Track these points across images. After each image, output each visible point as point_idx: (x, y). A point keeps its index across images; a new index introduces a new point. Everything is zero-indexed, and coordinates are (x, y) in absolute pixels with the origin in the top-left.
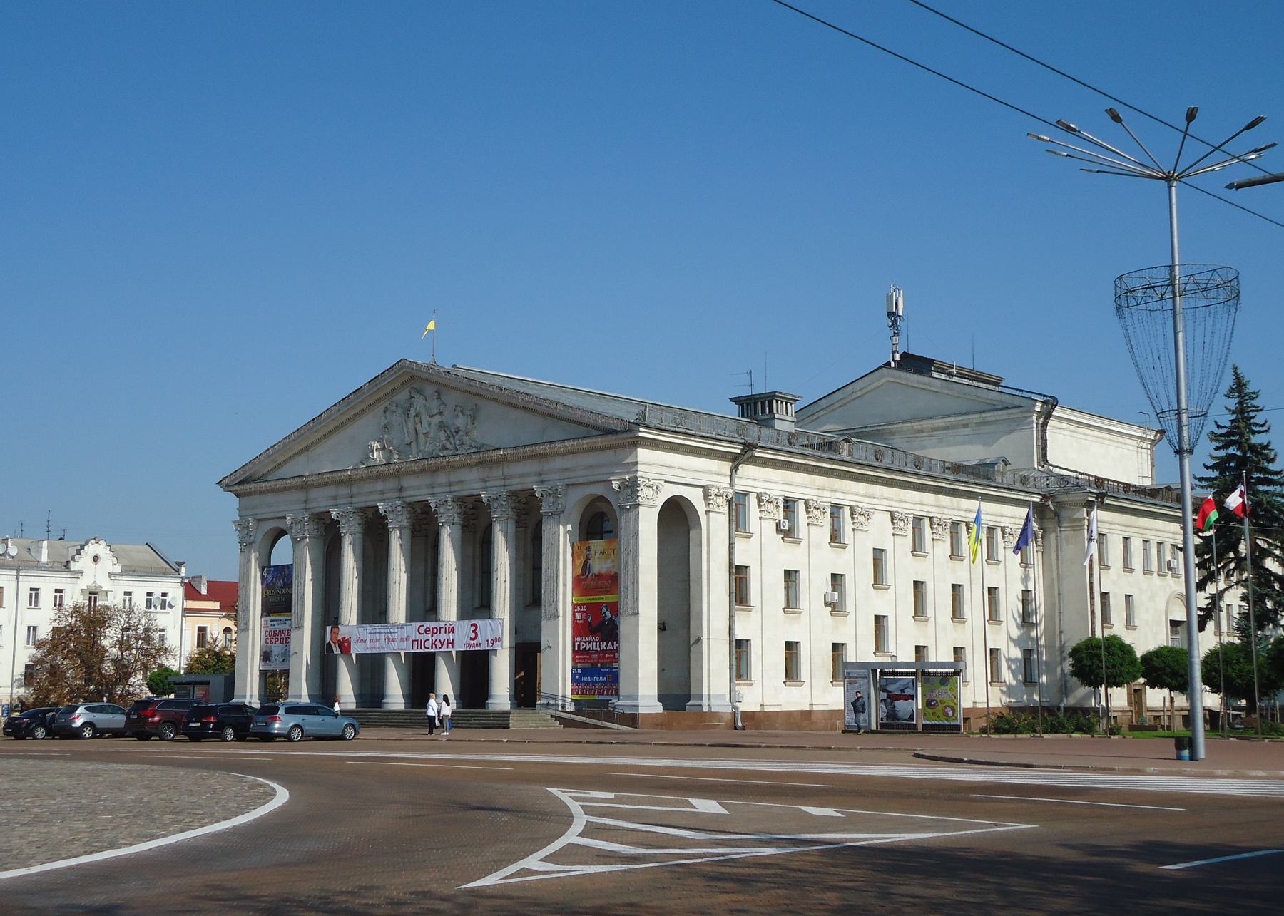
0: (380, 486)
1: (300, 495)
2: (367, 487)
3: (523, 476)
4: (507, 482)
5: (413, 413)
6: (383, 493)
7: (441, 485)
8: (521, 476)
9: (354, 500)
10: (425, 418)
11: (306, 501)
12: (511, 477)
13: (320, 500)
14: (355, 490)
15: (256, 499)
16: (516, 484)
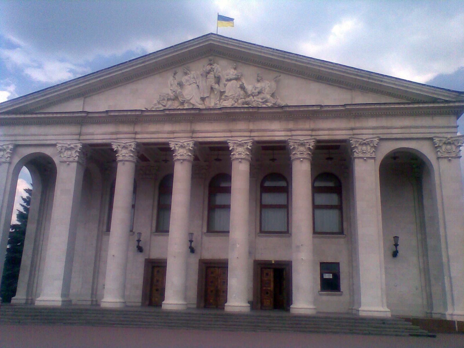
0: (168, 127)
1: (74, 129)
2: (152, 128)
3: (334, 130)
4: (314, 133)
5: (212, 75)
6: (173, 132)
7: (240, 131)
8: (329, 129)
9: (138, 136)
10: (223, 81)
11: (80, 134)
12: (319, 130)
13: (98, 134)
14: (138, 129)
15: (19, 130)
16: (324, 135)
